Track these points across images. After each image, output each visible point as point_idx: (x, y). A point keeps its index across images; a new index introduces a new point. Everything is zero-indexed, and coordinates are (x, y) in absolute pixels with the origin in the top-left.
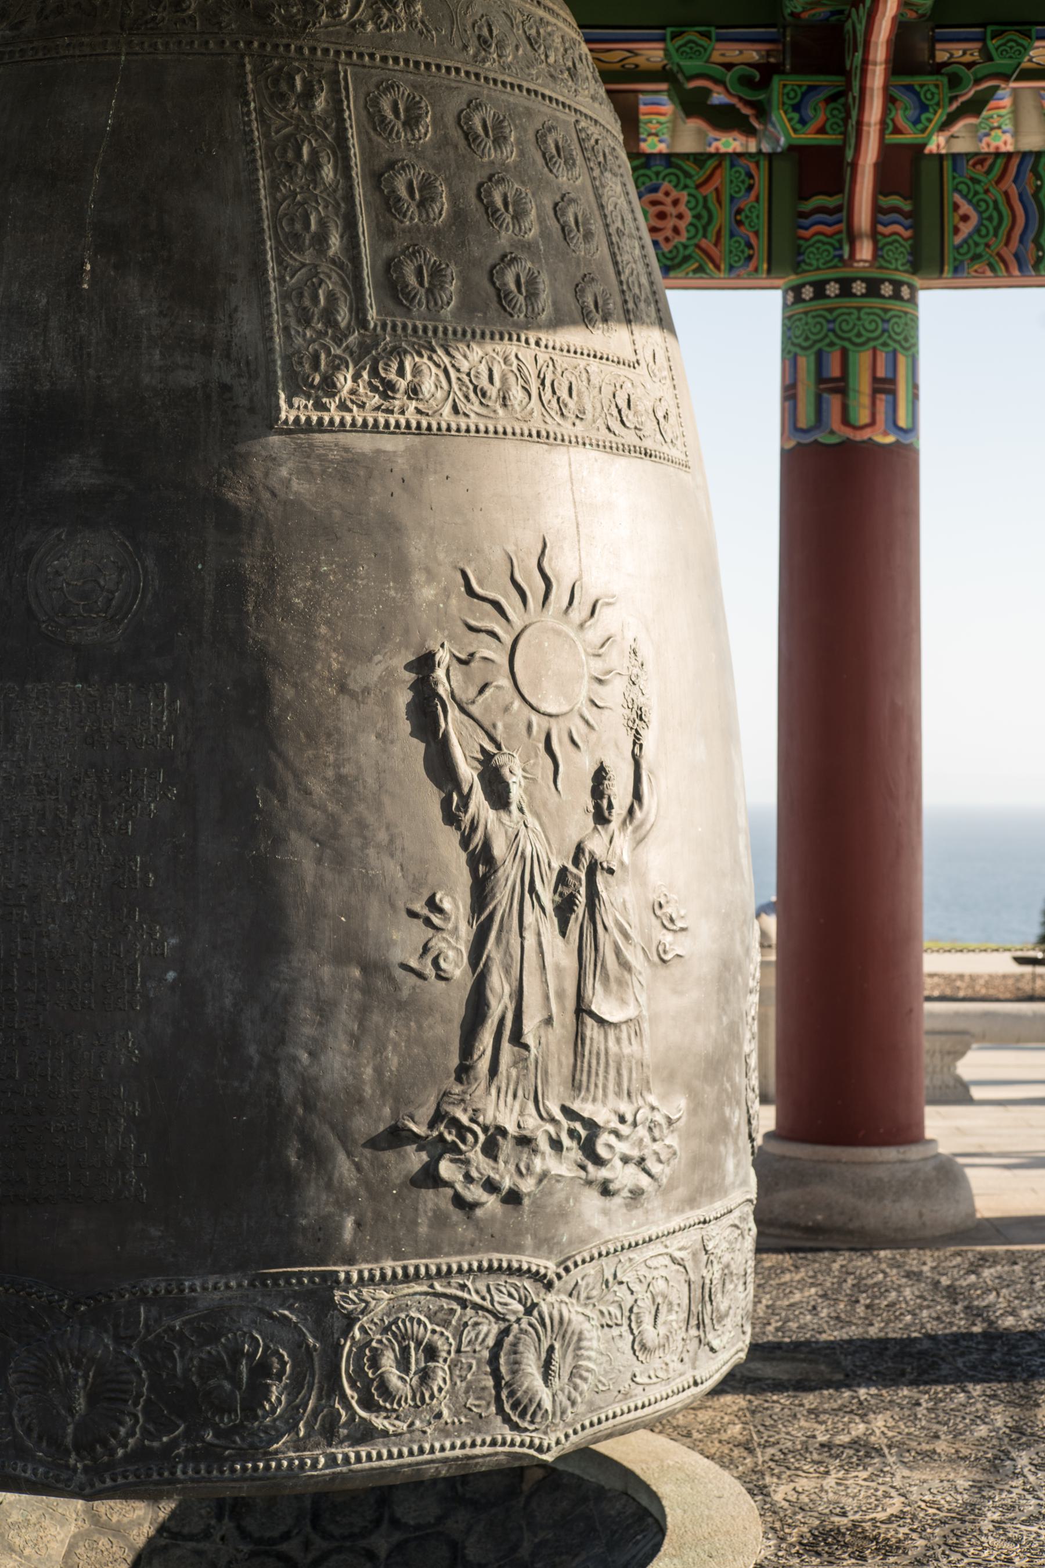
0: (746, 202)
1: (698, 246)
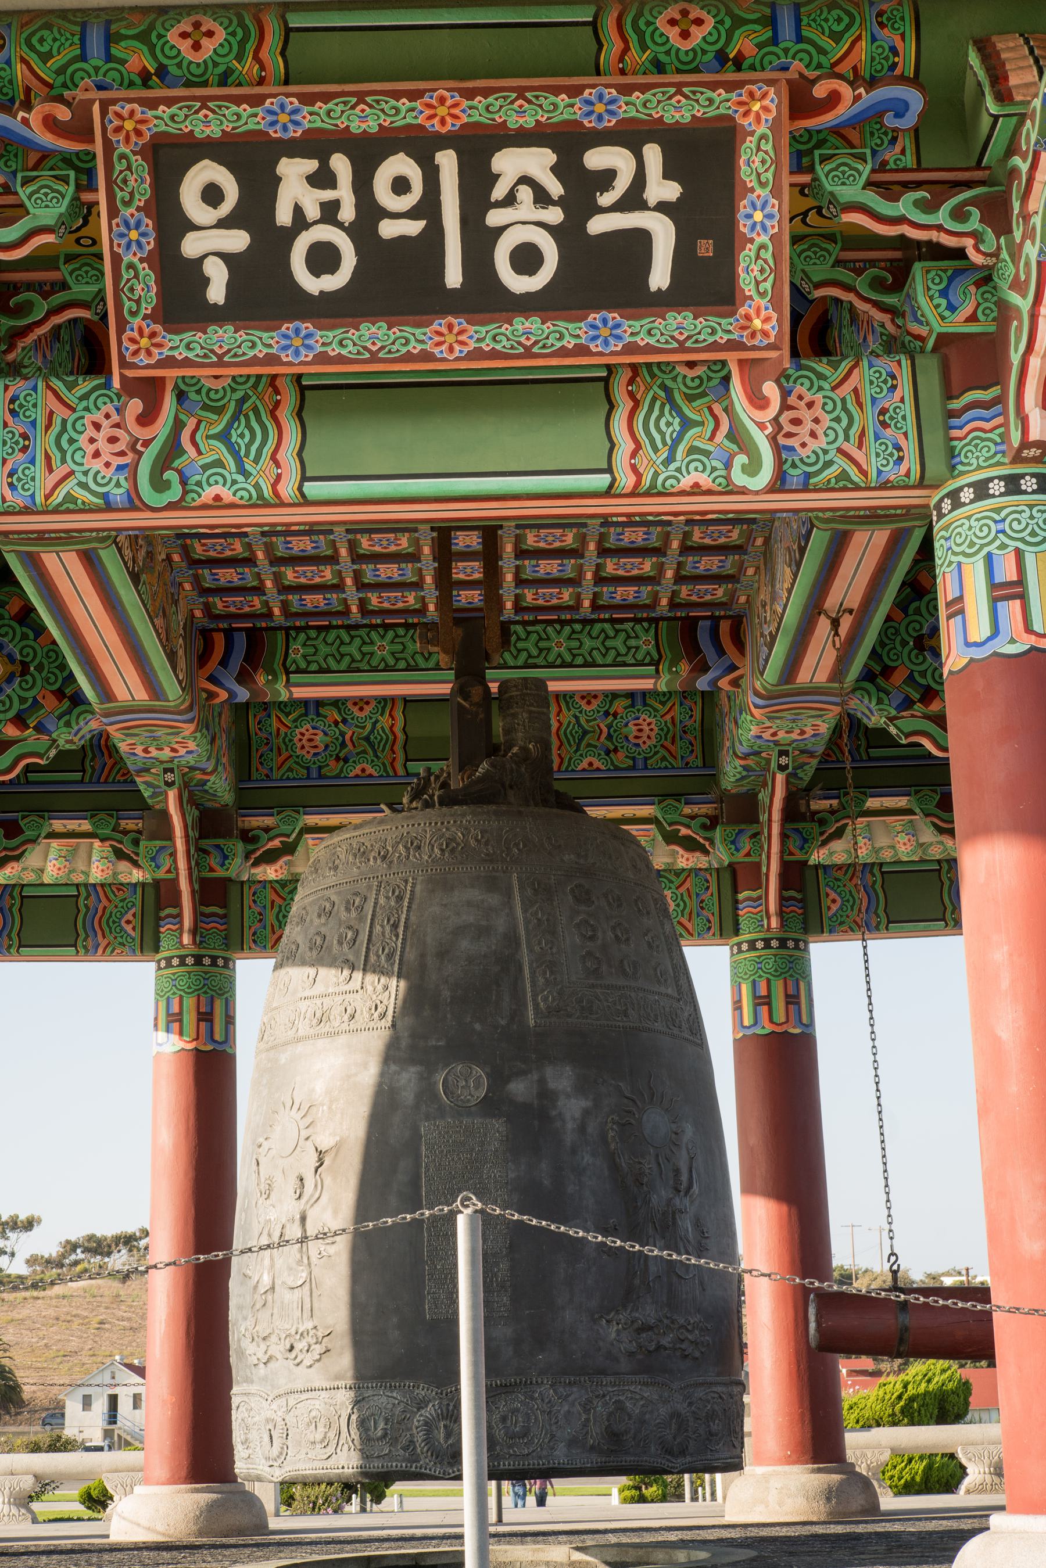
0: (890, 402)
1: (840, 450)
